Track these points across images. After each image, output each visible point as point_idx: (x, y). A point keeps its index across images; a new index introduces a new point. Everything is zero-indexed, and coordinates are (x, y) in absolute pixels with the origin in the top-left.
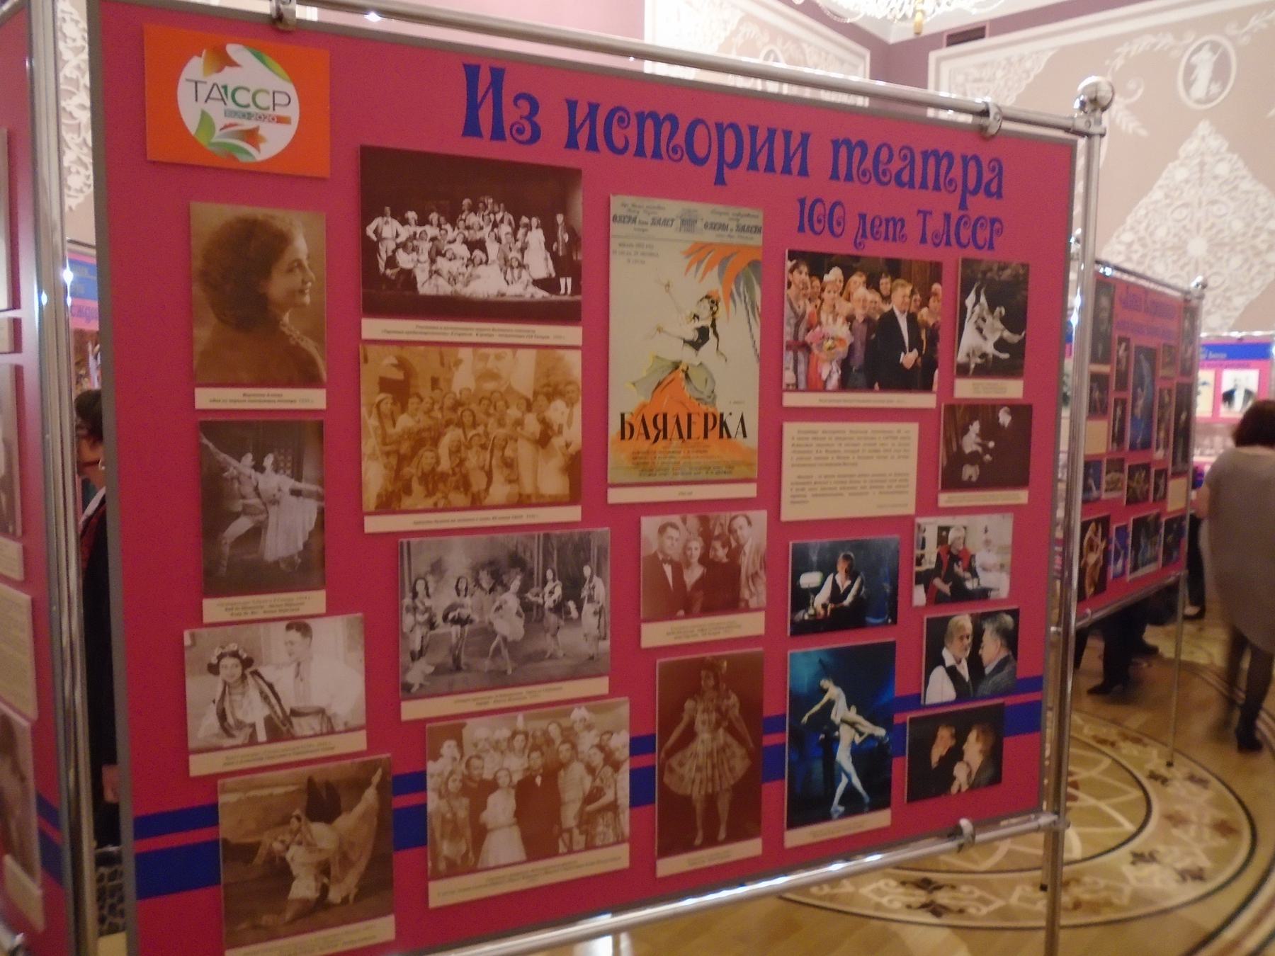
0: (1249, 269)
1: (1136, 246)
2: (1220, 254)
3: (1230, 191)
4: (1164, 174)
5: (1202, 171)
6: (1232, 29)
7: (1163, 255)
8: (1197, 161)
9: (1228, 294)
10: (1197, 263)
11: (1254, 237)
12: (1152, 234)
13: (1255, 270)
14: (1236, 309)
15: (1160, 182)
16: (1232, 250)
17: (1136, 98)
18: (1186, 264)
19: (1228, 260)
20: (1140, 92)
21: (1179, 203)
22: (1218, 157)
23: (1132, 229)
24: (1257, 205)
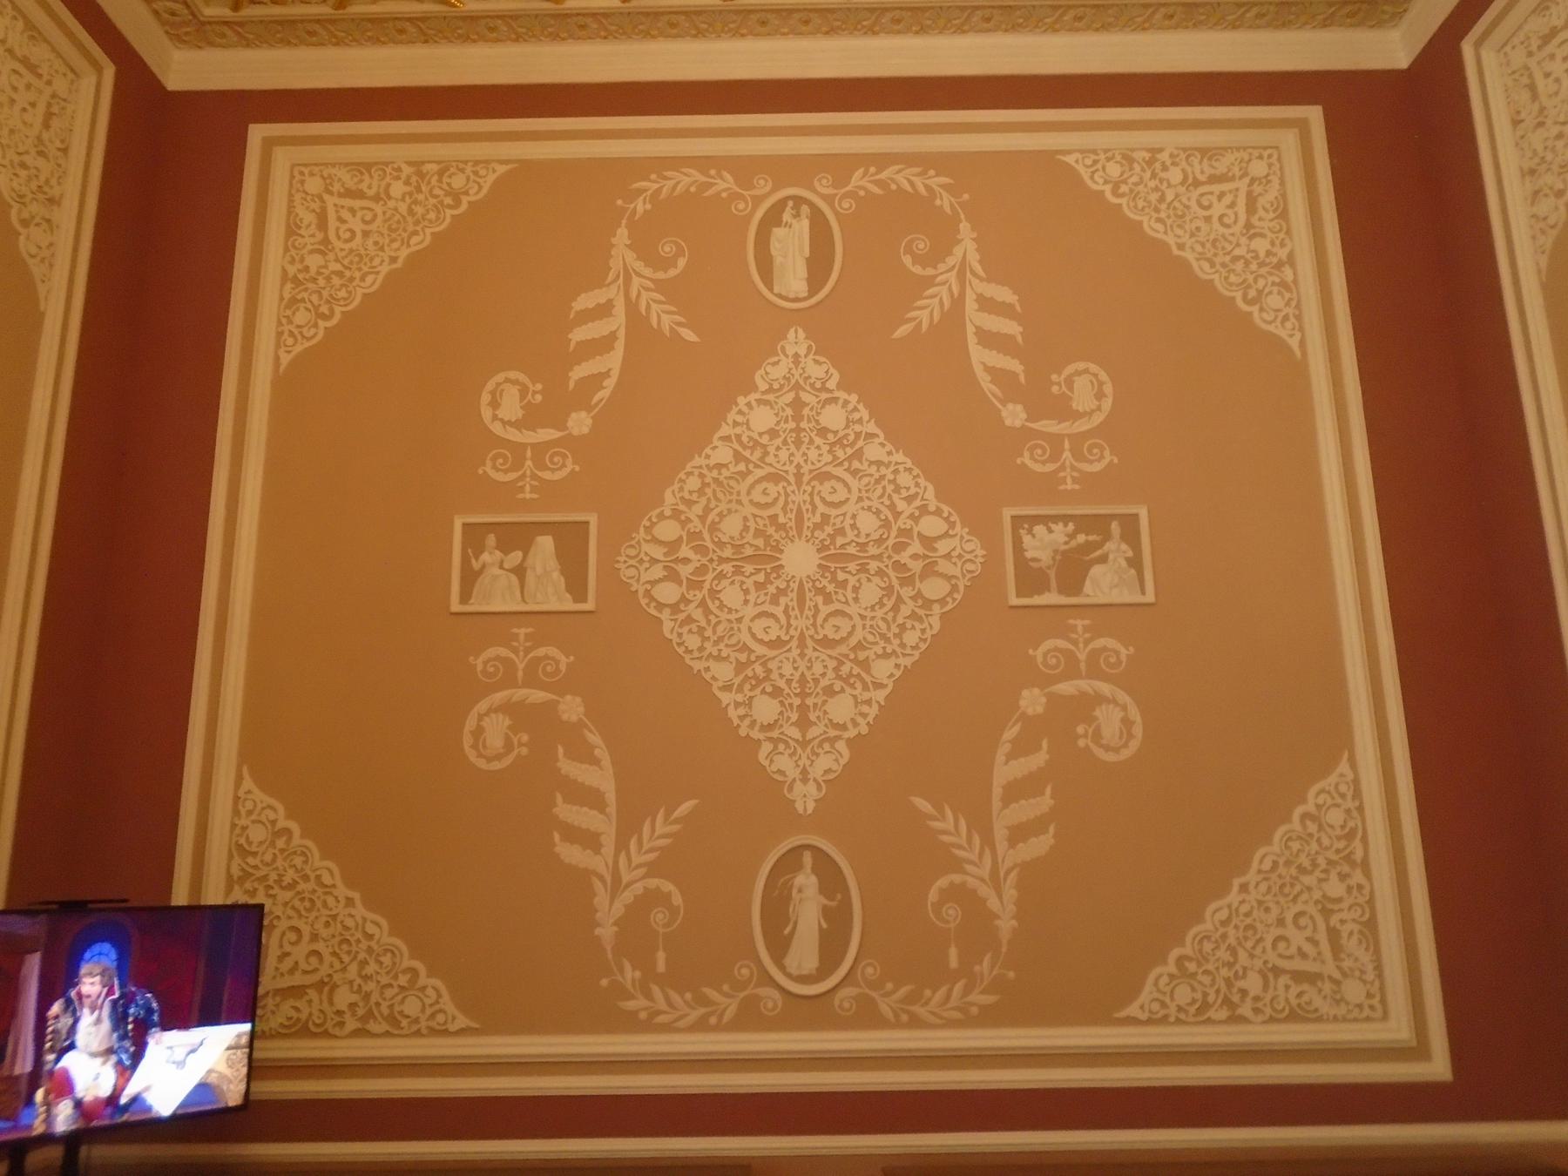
0: (896, 609)
1: (685, 551)
2: (841, 576)
3: (850, 459)
4: (732, 416)
5: (798, 418)
6: (824, 185)
7: (738, 571)
8: (790, 397)
9: (862, 656)
10: (801, 585)
11: (899, 547)
12: (714, 528)
13: (905, 610)
14: (879, 686)
15: (725, 430)
16: (863, 568)
17: (672, 273)
18: (782, 592)
19: (856, 589)
20: (682, 263)
21: (759, 473)
22: (824, 396)
23: (676, 514)
24: (897, 489)
